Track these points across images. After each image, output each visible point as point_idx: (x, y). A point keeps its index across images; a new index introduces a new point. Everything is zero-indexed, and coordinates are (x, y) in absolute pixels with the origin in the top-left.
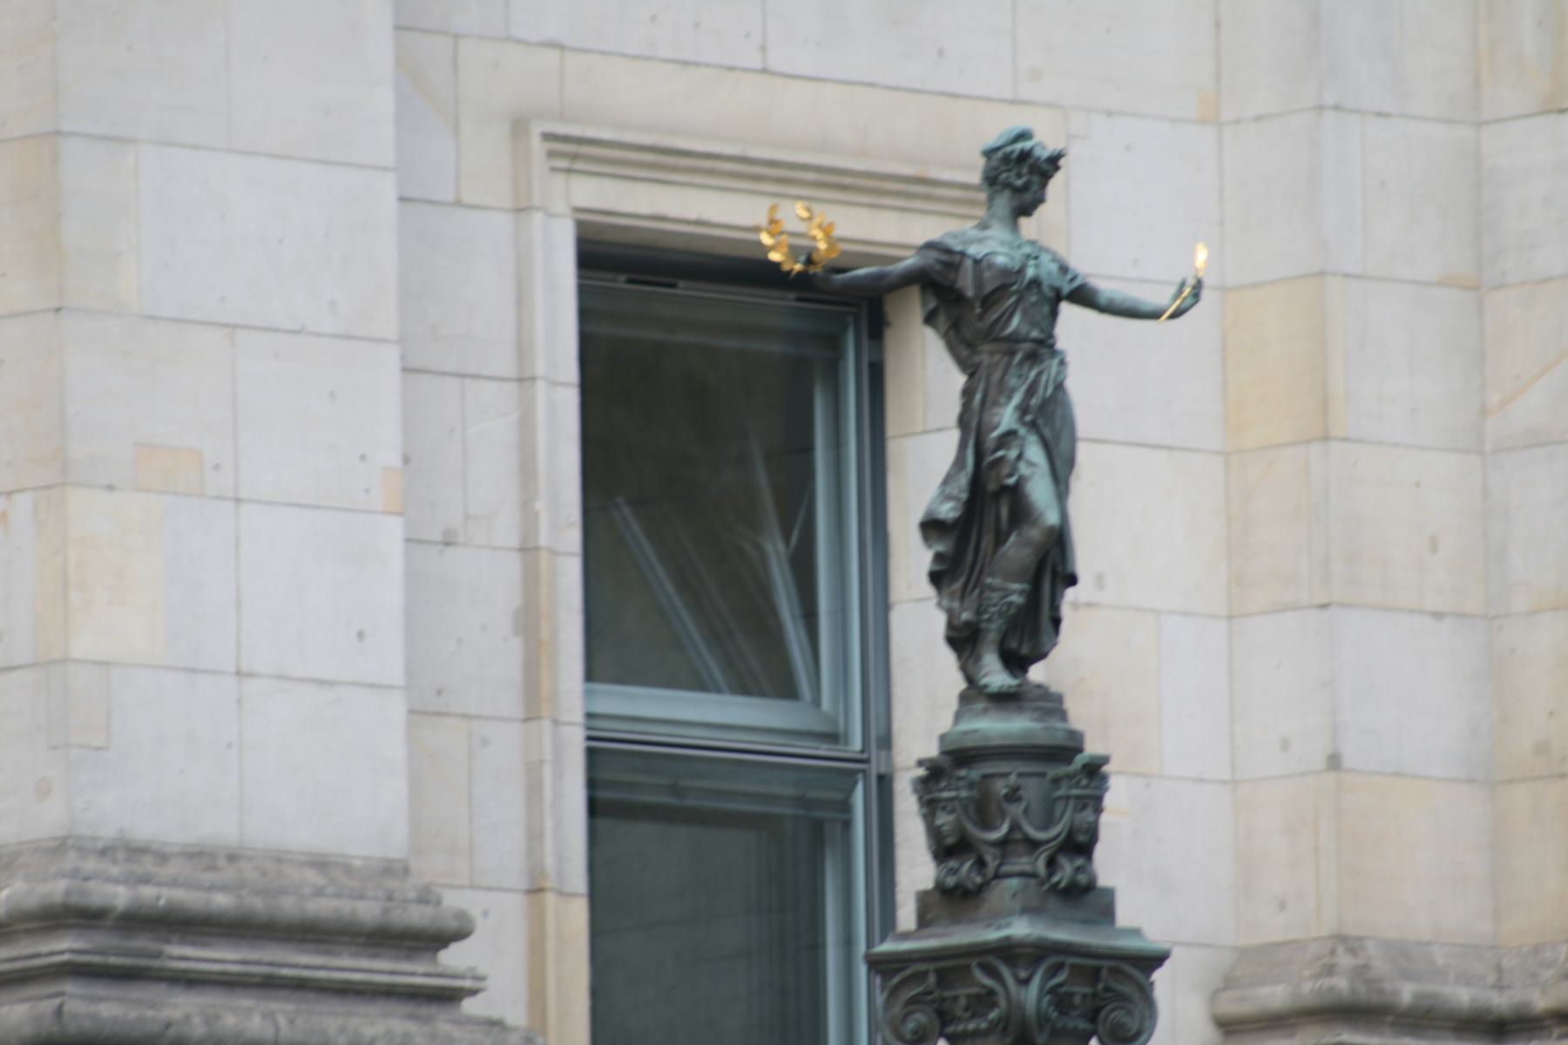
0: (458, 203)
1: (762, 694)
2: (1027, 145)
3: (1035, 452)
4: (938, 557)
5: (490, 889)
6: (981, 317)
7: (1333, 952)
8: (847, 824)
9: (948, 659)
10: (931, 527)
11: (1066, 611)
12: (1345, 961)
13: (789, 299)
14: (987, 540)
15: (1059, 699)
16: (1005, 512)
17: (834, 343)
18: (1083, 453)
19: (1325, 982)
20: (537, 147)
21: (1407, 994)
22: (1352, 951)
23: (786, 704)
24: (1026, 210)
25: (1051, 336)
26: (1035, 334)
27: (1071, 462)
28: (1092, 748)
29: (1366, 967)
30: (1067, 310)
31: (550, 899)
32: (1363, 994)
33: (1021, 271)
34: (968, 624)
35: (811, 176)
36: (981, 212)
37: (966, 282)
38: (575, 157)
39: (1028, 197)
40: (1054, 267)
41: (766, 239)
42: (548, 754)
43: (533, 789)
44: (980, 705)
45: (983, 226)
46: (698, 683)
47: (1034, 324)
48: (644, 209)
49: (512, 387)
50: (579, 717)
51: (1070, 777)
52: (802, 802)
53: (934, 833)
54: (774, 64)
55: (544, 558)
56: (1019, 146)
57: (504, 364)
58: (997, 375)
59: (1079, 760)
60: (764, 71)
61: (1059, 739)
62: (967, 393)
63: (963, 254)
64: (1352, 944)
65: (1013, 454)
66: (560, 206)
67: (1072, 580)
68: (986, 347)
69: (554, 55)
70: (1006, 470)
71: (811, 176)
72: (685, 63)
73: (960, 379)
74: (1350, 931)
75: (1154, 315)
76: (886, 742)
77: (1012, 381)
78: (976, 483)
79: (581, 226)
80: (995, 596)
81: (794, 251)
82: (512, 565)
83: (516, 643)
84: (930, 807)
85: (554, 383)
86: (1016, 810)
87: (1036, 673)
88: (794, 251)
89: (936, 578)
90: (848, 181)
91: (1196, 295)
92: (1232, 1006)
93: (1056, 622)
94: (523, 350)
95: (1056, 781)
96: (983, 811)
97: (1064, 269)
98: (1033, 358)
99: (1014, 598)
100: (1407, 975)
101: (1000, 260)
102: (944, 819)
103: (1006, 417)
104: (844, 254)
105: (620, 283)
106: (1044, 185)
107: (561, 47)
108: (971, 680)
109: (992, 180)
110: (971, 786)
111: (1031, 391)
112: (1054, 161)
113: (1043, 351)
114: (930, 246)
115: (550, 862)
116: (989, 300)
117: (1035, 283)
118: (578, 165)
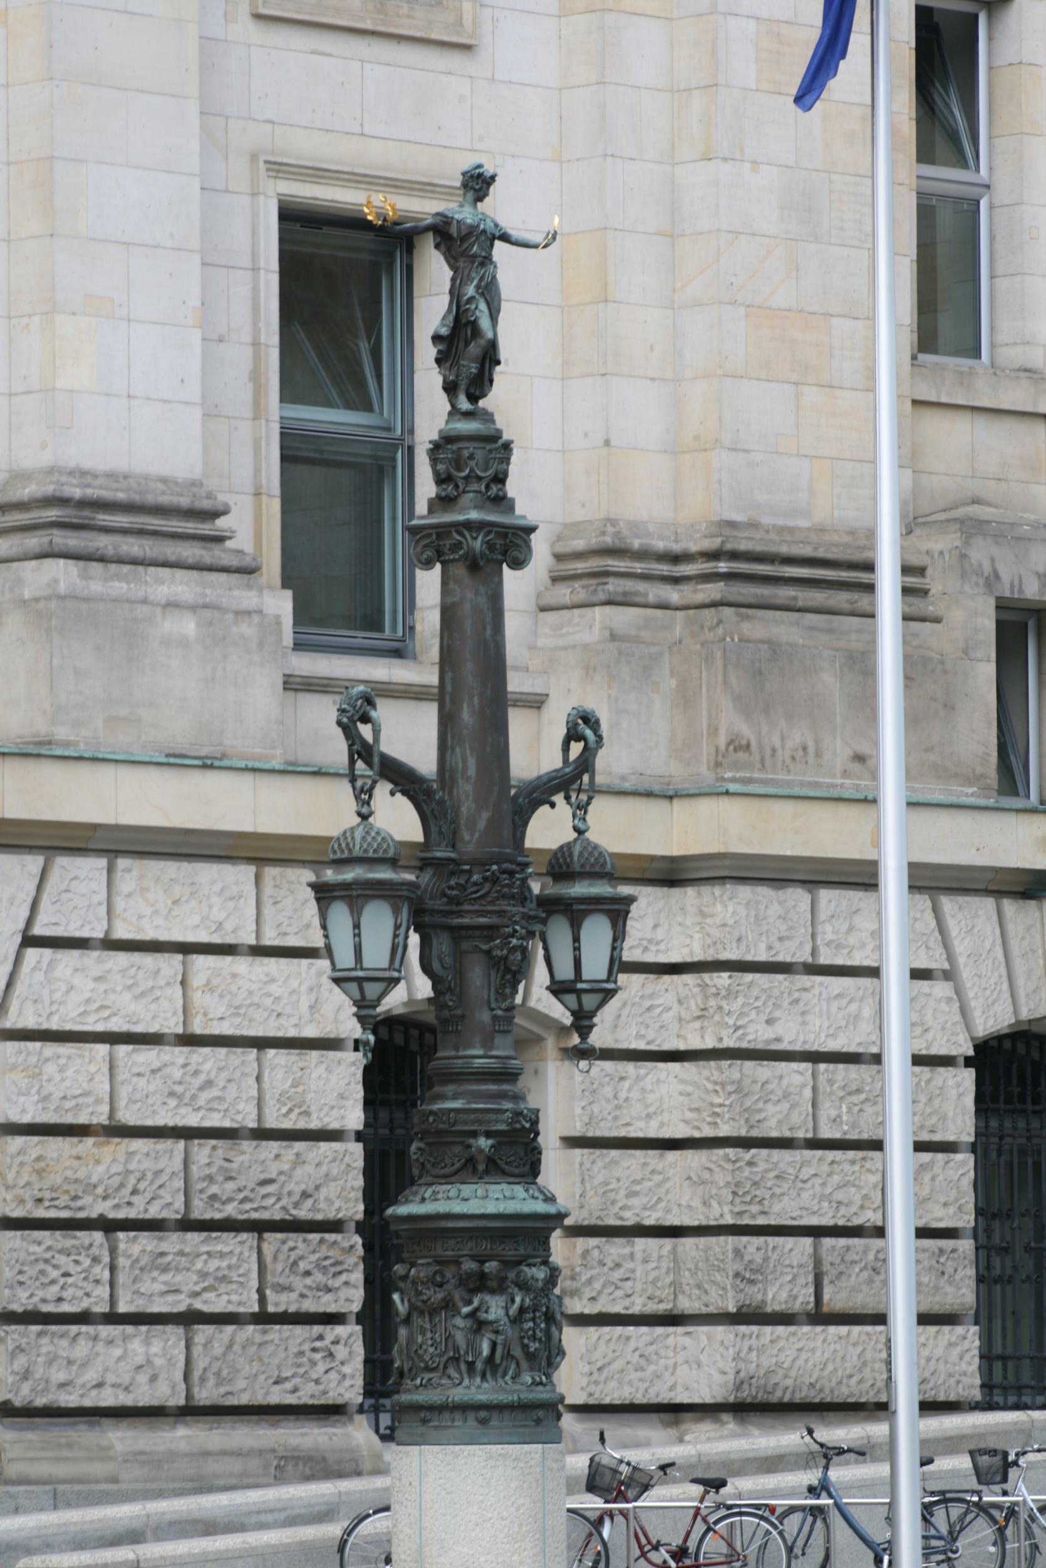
0: (227, 191)
1: (357, 409)
2: (481, 170)
3: (483, 306)
4: (439, 352)
5: (238, 493)
6: (460, 246)
7: (605, 526)
8: (394, 467)
9: (443, 396)
10: (436, 338)
11: (496, 377)
12: (610, 529)
13: (371, 236)
14: (461, 344)
15: (492, 415)
16: (469, 332)
17: (391, 255)
18: (503, 305)
19: (601, 539)
20: (262, 166)
21: (636, 544)
22: (613, 526)
23: (366, 414)
24: (480, 199)
25: (490, 254)
26: (483, 254)
27: (499, 311)
28: (506, 437)
29: (619, 532)
30: (497, 243)
31: (264, 498)
32: (618, 544)
33: (478, 226)
34: (452, 381)
35: (382, 181)
36: (461, 199)
37: (454, 231)
38: (278, 171)
39: (481, 193)
40: (492, 225)
41: (366, 210)
42: (263, 435)
43: (257, 450)
44: (457, 417)
45: (461, 206)
46: (328, 404)
47: (483, 249)
48: (308, 195)
49: (249, 273)
50: (277, 418)
51: (496, 449)
52: (375, 457)
53: (437, 474)
54: (367, 131)
55: (263, 348)
56: (477, 171)
57: (246, 262)
58: (466, 273)
59: (500, 442)
60: (362, 134)
61: (492, 433)
62: (453, 280)
63: (452, 218)
64: (612, 522)
65: (473, 307)
66: (272, 193)
67: (498, 363)
68: (462, 260)
69: (271, 125)
70: (470, 314)
71: (382, 181)
72: (327, 131)
73: (449, 273)
74: (613, 517)
75: (536, 247)
76: (412, 431)
77: (473, 274)
78: (457, 320)
79: (280, 201)
80: (465, 369)
81: (378, 215)
82: (249, 351)
83: (250, 386)
84: (434, 461)
85: (268, 271)
86: (473, 463)
87: (482, 403)
88: (378, 215)
89: (438, 361)
90: (398, 184)
91: (554, 238)
92: (561, 549)
93: (491, 381)
94: (254, 256)
95: (490, 451)
96: (458, 464)
97: (496, 225)
98: (482, 264)
99: (473, 370)
100: (637, 536)
101: (469, 221)
102: (441, 467)
103: (470, 290)
104: (400, 216)
105: (298, 227)
106: (488, 188)
107: (273, 123)
108: (453, 406)
109: (465, 185)
110: (453, 452)
111: (482, 279)
112: (493, 178)
113: (487, 261)
114: (438, 214)
115: (264, 482)
116: (463, 239)
117: (484, 231)
118: (280, 175)
